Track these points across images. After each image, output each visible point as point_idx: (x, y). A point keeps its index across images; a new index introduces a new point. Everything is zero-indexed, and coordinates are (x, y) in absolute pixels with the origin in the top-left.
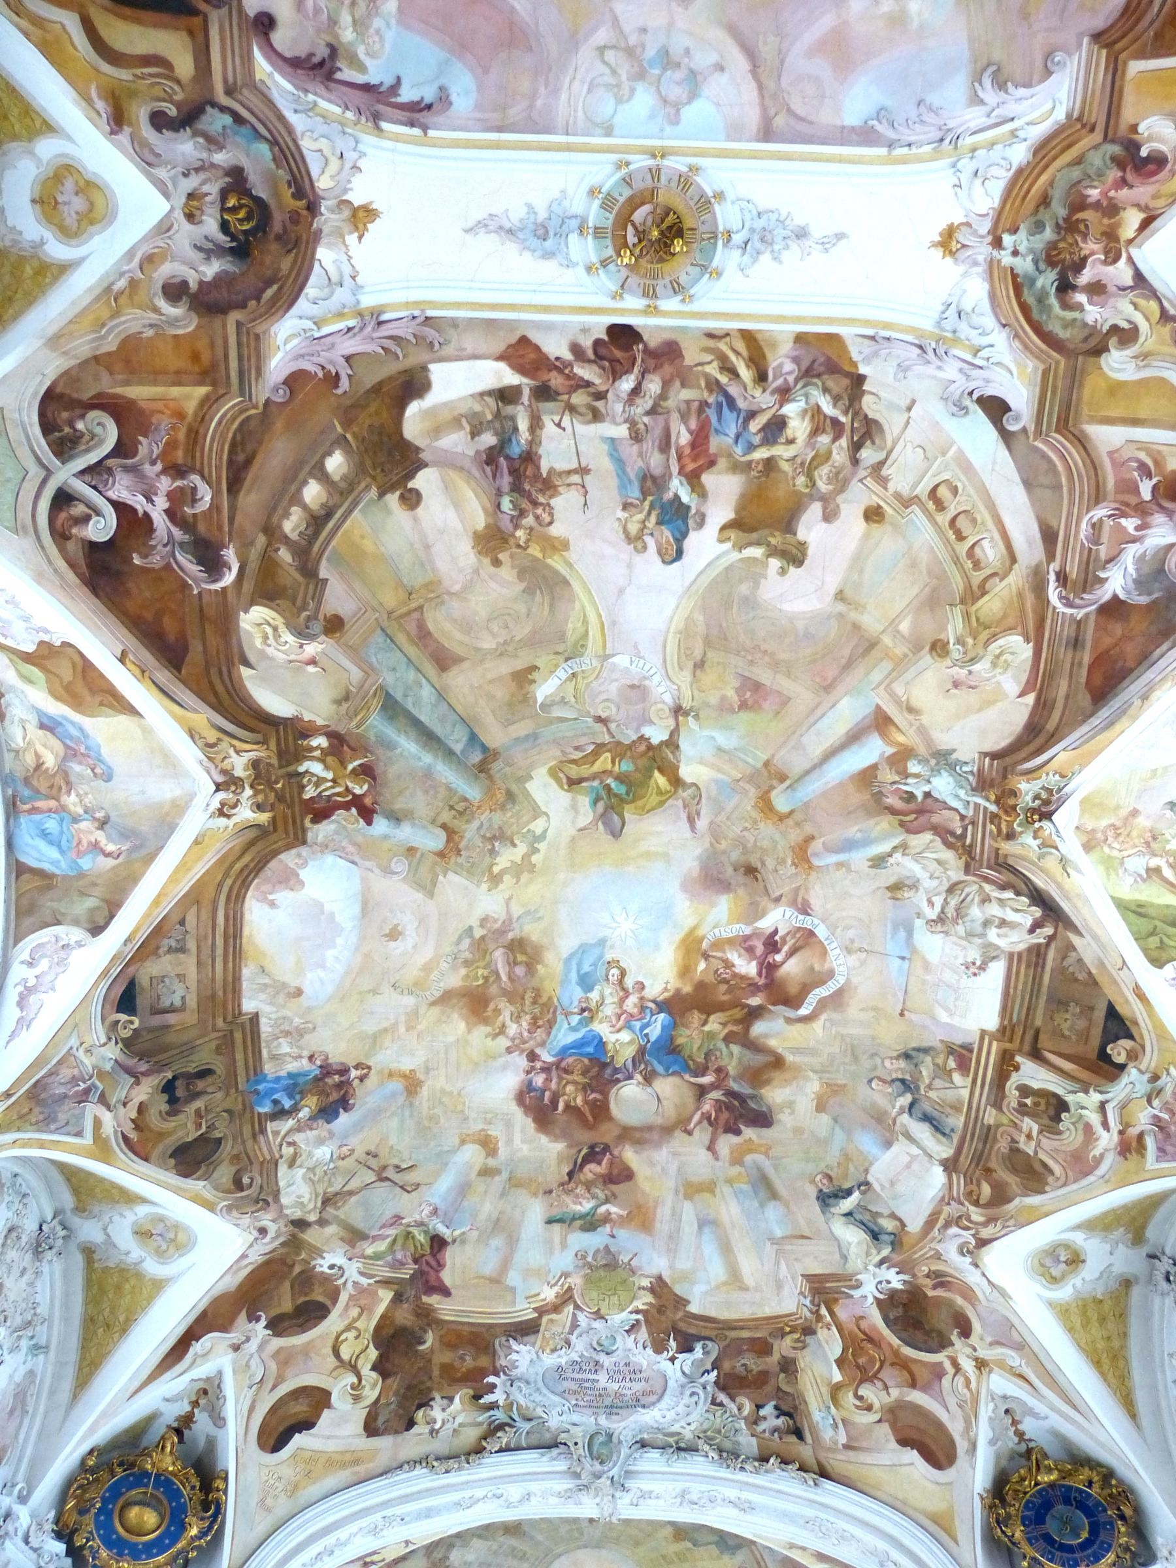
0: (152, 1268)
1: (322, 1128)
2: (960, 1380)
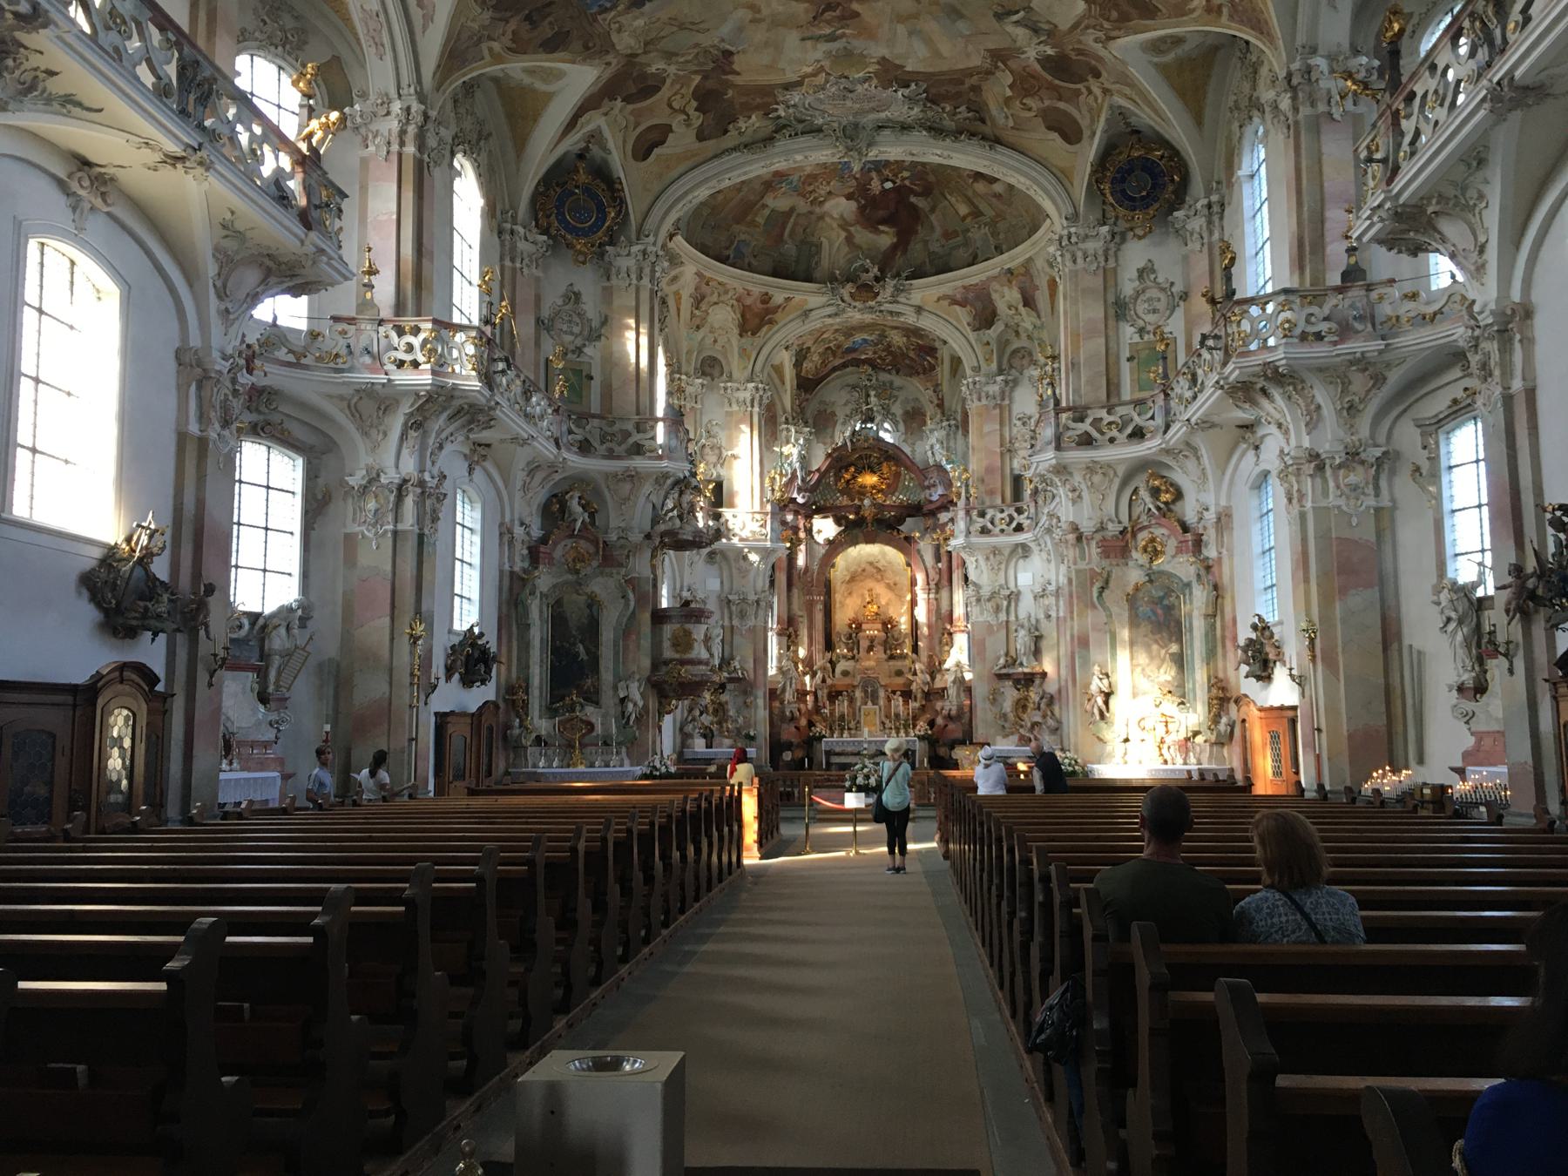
0: (540, 86)
1: (636, 12)
2: (1091, 98)
